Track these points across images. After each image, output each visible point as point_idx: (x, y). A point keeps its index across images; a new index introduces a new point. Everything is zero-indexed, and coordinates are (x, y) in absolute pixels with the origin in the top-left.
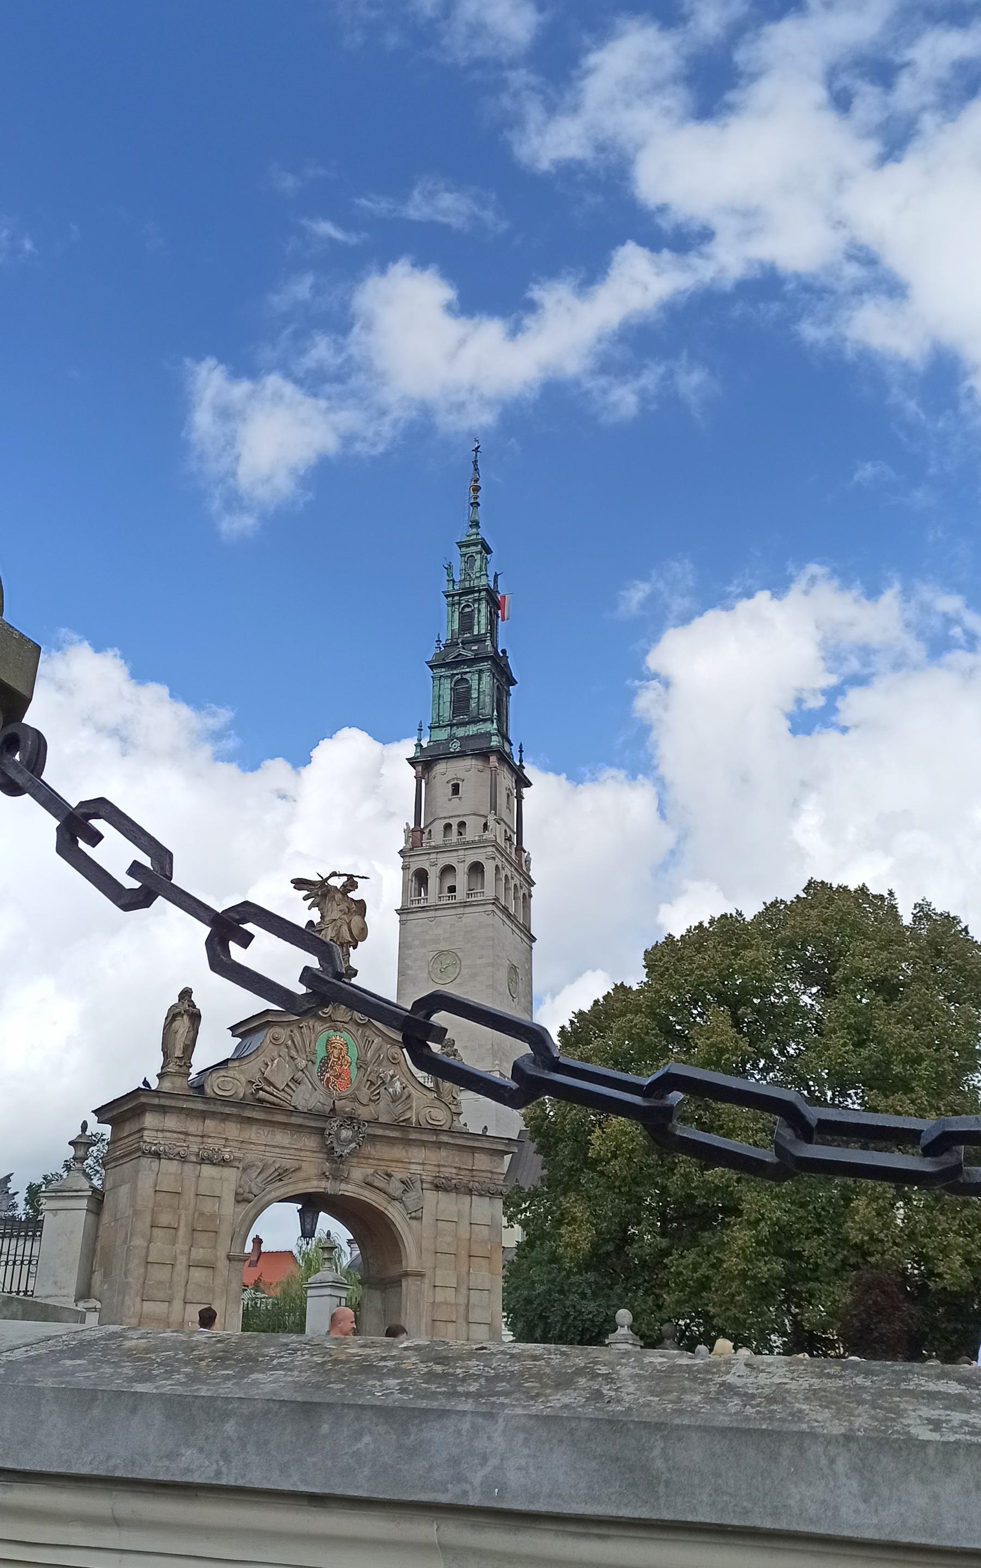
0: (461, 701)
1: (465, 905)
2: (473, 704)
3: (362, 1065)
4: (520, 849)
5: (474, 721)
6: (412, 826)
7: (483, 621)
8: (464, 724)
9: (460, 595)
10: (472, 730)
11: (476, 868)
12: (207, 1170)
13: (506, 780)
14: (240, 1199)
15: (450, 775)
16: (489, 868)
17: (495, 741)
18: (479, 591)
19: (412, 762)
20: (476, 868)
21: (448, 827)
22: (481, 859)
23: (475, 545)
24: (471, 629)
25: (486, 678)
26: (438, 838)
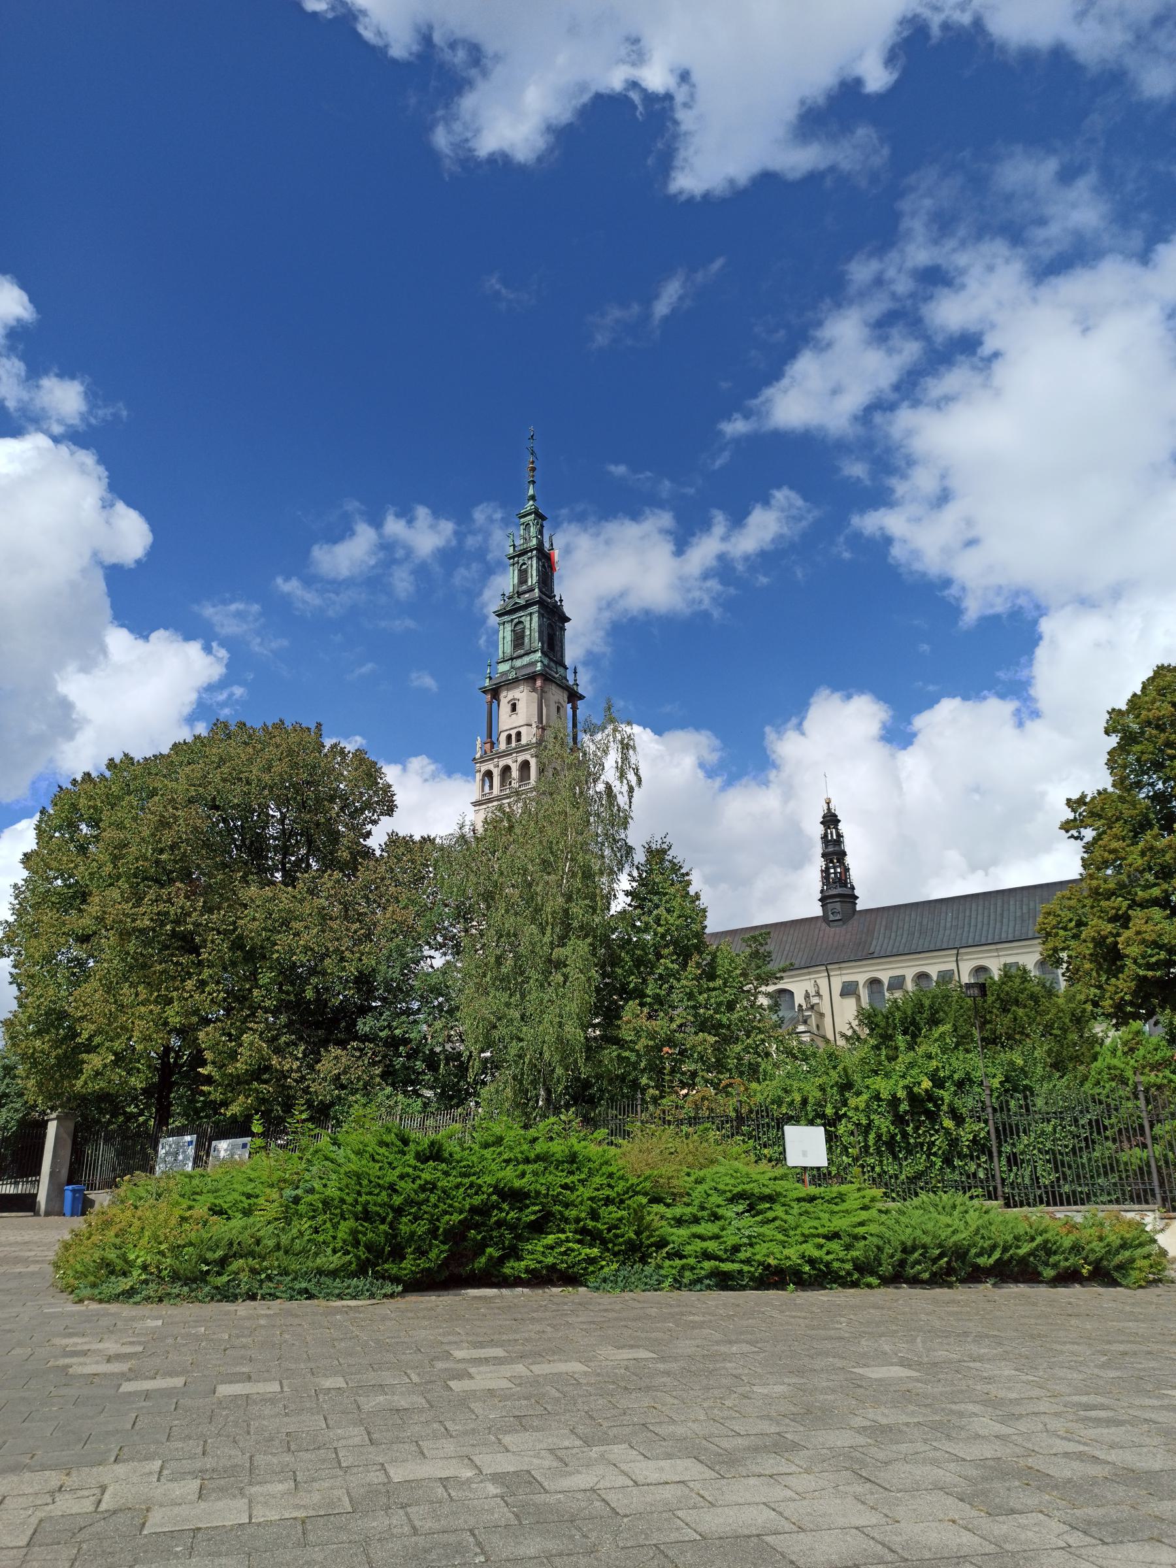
2: (527, 640)
5: (527, 654)
7: (534, 574)
9: (519, 556)
10: (526, 660)
11: (525, 765)
15: (510, 697)
16: (533, 762)
18: (531, 551)
20: (525, 765)
21: (509, 737)
22: (528, 757)
23: (530, 514)
24: (526, 581)
25: (535, 617)
26: (503, 746)
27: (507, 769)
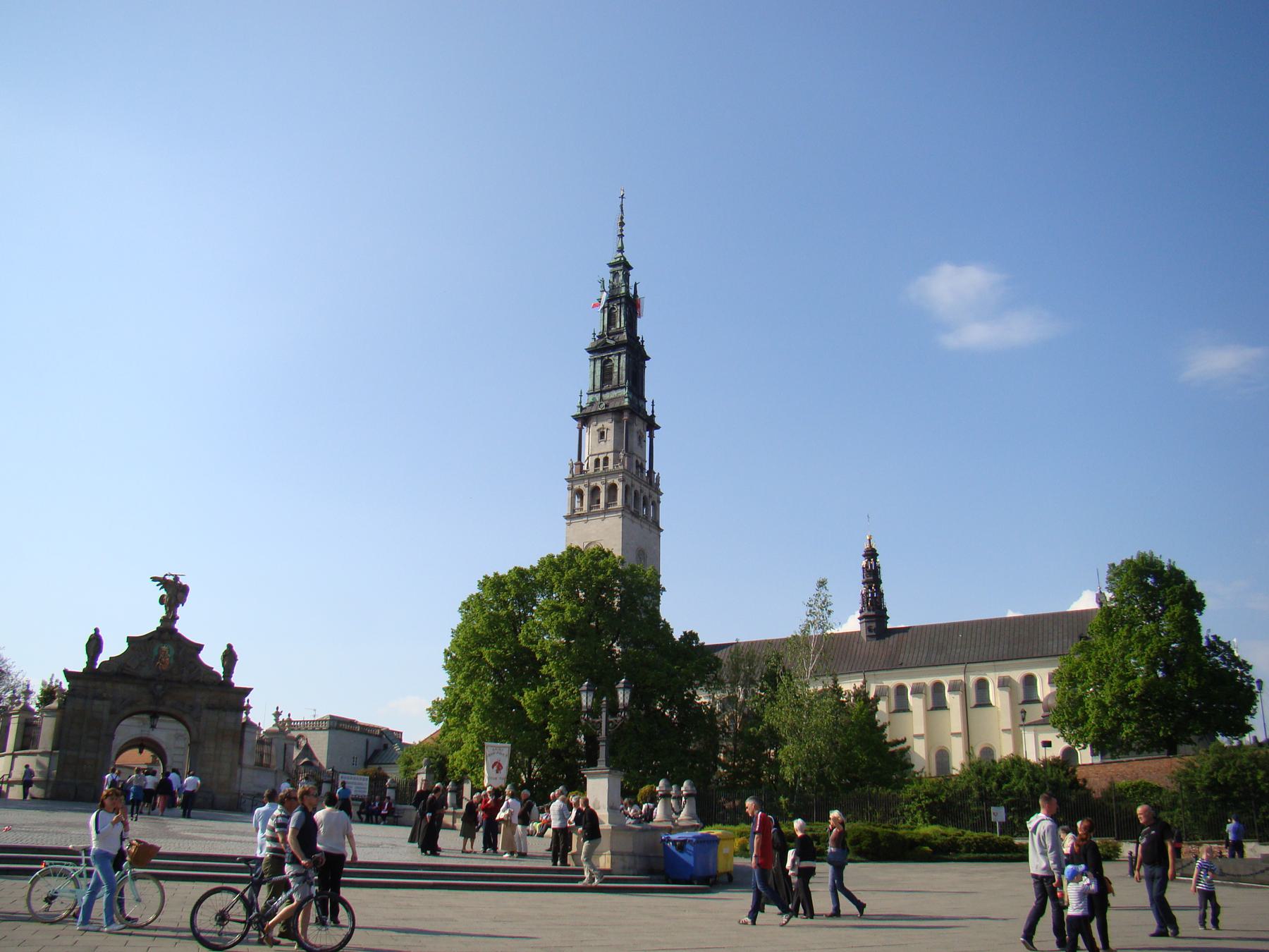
0: (606, 375)
1: (606, 512)
2: (615, 377)
3: (176, 658)
4: (651, 472)
6: (575, 460)
8: (609, 390)
10: (614, 394)
11: (612, 489)
12: (97, 702)
13: (639, 425)
14: (112, 712)
15: (600, 425)
16: (620, 487)
17: (626, 402)
19: (576, 418)
20: (612, 489)
21: (597, 461)
22: (616, 481)
24: (614, 324)
25: (623, 358)
27: (595, 490)
